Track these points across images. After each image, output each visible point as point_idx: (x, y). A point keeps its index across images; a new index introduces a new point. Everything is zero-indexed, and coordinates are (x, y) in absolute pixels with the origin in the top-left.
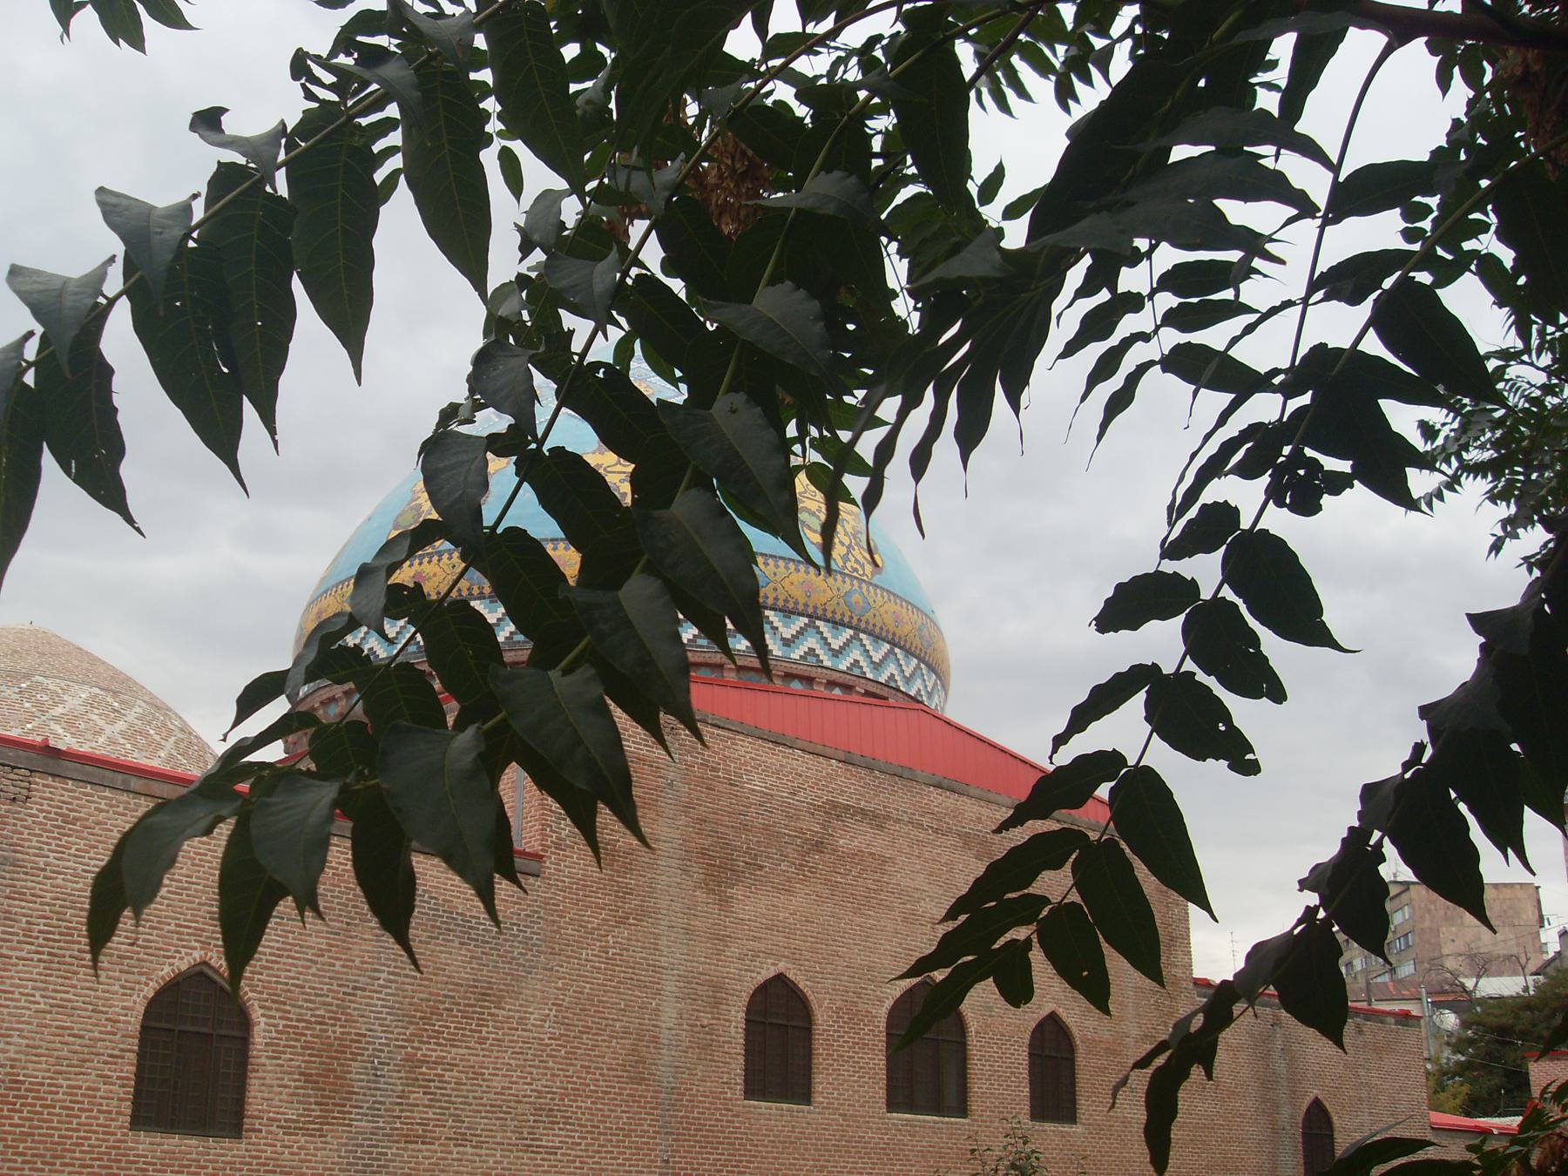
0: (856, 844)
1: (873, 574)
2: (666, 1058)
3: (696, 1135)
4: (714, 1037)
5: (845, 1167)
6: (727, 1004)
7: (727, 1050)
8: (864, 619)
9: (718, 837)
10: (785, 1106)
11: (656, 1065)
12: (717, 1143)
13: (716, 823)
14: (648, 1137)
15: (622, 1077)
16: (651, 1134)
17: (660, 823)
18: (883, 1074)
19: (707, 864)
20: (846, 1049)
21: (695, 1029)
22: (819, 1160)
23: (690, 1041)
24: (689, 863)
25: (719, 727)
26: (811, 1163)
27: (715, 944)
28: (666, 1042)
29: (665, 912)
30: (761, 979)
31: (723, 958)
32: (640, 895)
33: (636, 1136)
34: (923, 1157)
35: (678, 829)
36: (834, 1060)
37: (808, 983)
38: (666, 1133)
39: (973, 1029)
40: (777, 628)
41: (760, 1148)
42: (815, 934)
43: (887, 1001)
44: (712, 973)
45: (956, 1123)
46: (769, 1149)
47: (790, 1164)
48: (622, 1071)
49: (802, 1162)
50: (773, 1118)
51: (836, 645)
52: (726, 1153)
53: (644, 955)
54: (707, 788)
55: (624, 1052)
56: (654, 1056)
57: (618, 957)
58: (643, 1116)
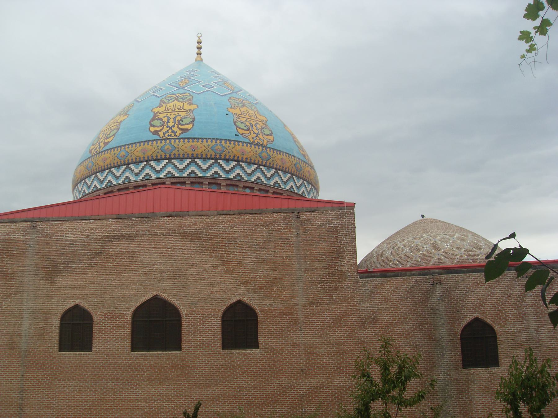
0: (119, 249)
1: (180, 134)
2: (23, 340)
3: (36, 366)
4: (45, 331)
5: (108, 374)
6: (51, 319)
7: (50, 335)
8: (172, 154)
9: (51, 260)
10: (77, 353)
11: (19, 343)
12: (45, 368)
13: (50, 256)
14: (16, 368)
15: (6, 348)
16: (17, 367)
17: (26, 260)
18: (129, 337)
19: (46, 271)
20: (109, 329)
21: (36, 329)
22: (94, 372)
23: (34, 334)
24: (38, 272)
25: (55, 221)
26: (90, 373)
27: (47, 298)
28: (24, 335)
29: (26, 290)
30: (67, 308)
31: (50, 302)
32: (16, 287)
33: (11, 368)
34: (151, 368)
35: (33, 261)
36: (103, 334)
37: (90, 306)
38: (24, 366)
39: (184, 314)
40: (133, 170)
41: (66, 369)
42: (95, 288)
43: (132, 308)
44: (45, 308)
45: (172, 354)
46: (70, 369)
47: (79, 374)
48: (6, 346)
49: (85, 373)
50: (71, 358)
51: (158, 168)
52: (49, 371)
53: (16, 306)
54: (46, 244)
55: (7, 340)
56: (19, 340)
57: (6, 309)
58: (14, 361)
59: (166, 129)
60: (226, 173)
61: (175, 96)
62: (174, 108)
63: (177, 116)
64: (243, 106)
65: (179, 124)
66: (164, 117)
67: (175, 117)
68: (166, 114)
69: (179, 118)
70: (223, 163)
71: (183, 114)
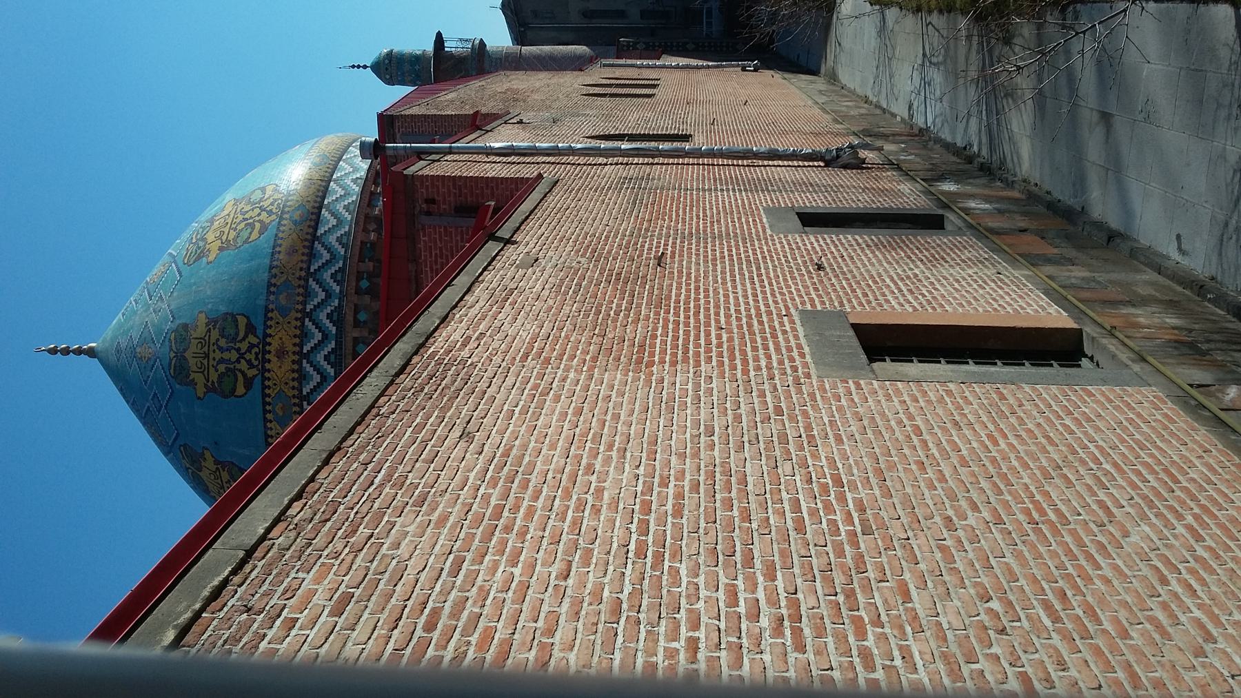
1: (255, 336)
59: (243, 365)
60: (334, 258)
61: (173, 362)
62: (197, 355)
63: (217, 345)
64: (203, 239)
65: (234, 340)
66: (217, 370)
67: (220, 348)
68: (211, 367)
69: (223, 343)
70: (316, 264)
71: (215, 334)
